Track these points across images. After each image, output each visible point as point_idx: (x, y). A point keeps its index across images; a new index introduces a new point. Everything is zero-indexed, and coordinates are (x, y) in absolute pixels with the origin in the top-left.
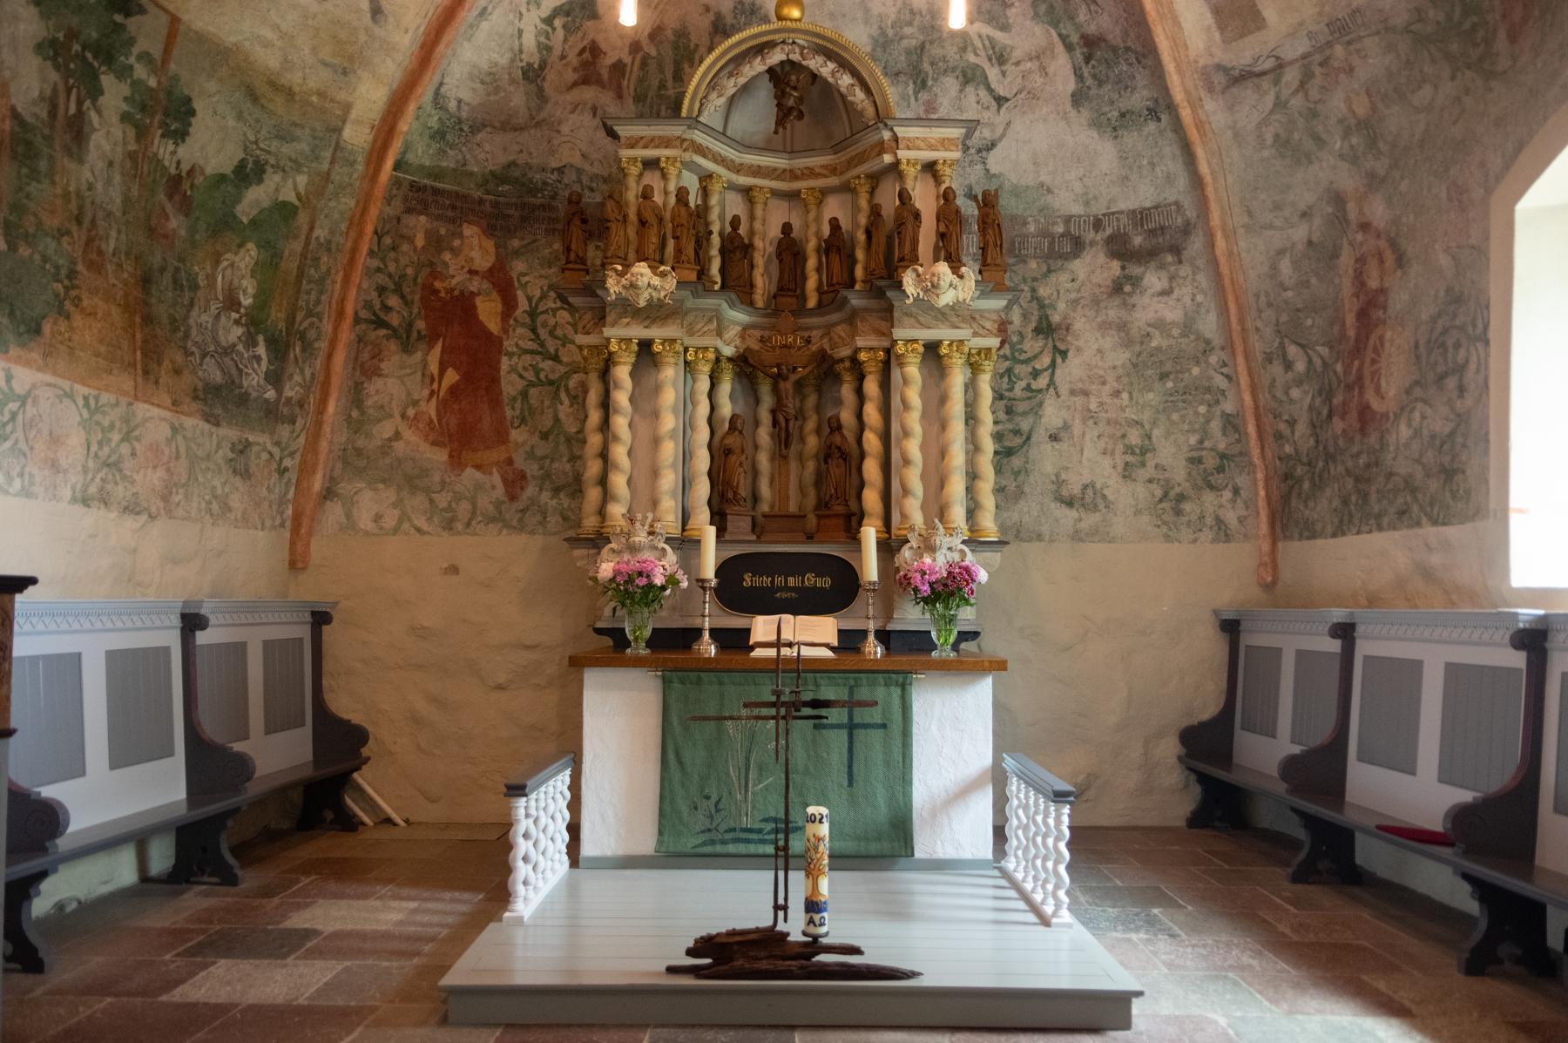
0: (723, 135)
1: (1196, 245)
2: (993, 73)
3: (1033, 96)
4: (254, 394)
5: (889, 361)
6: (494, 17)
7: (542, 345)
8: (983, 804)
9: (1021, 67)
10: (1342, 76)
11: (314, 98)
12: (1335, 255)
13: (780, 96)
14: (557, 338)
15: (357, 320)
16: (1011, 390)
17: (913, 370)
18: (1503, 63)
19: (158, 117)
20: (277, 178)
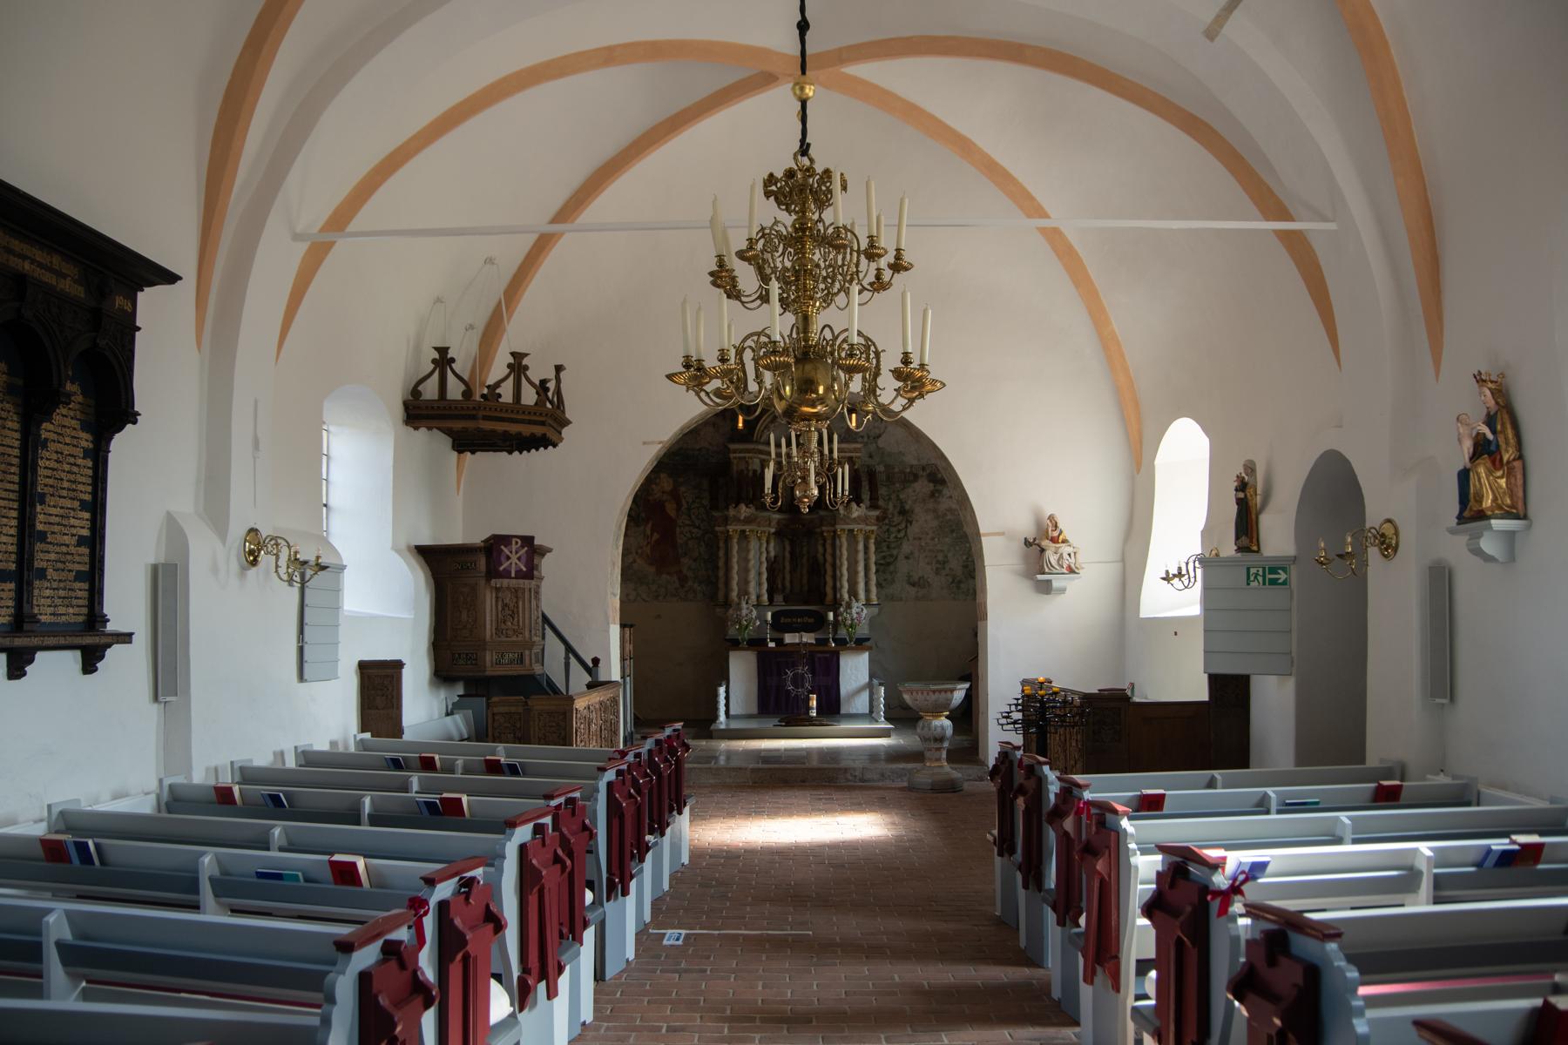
5: (835, 535)
8: (865, 695)
17: (844, 540)
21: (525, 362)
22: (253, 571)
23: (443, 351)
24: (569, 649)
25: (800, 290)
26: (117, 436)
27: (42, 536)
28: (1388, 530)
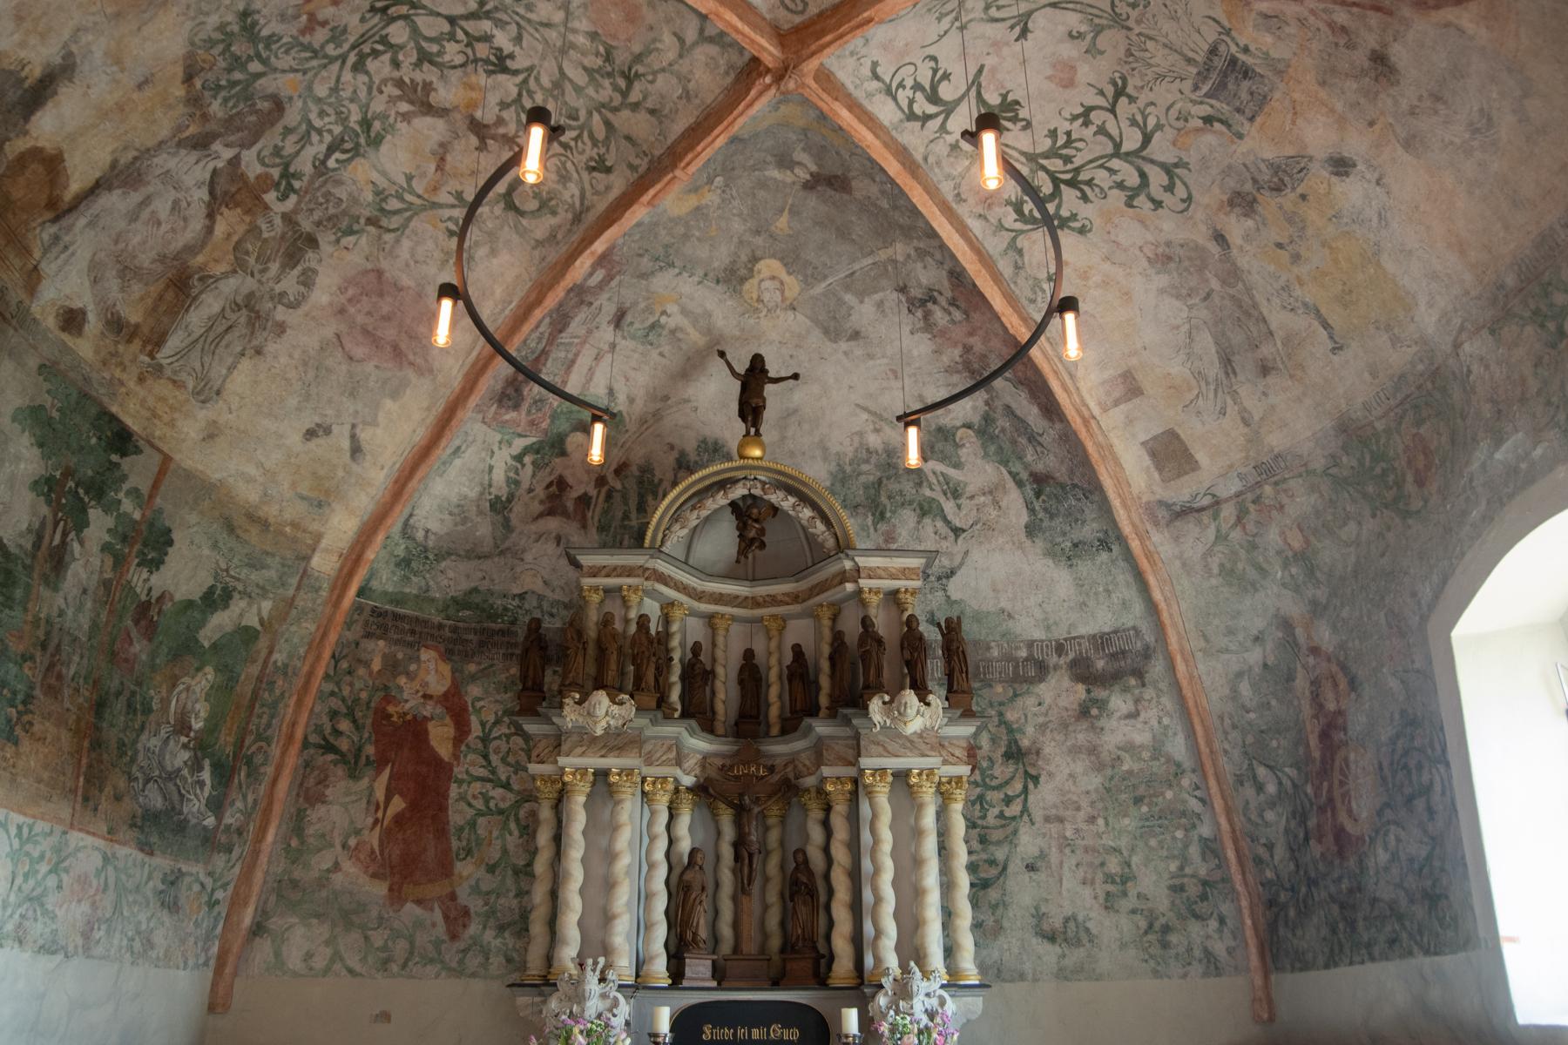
0: (686, 563)
1: (1157, 668)
2: (949, 507)
3: (989, 527)
4: (193, 821)
5: (857, 789)
6: (467, 455)
7: (493, 772)
9: (976, 501)
10: (1274, 513)
11: (288, 529)
12: (1290, 678)
13: (742, 528)
14: (509, 764)
15: (306, 744)
16: (984, 817)
18: (1416, 504)
19: (137, 547)
20: (243, 604)
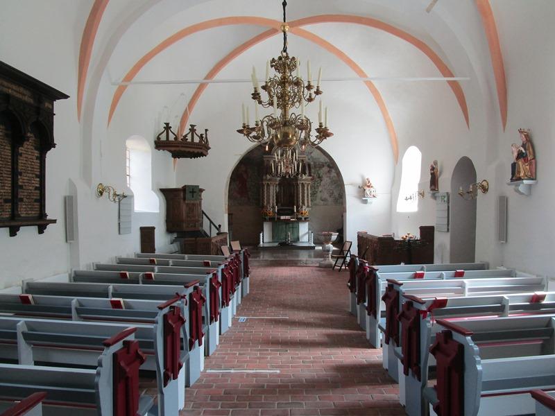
5: (297, 185)
8: (307, 236)
21: (195, 128)
22: (101, 198)
23: (167, 124)
24: (211, 222)
25: (283, 101)
26: (49, 152)
27: (21, 187)
28: (484, 183)
